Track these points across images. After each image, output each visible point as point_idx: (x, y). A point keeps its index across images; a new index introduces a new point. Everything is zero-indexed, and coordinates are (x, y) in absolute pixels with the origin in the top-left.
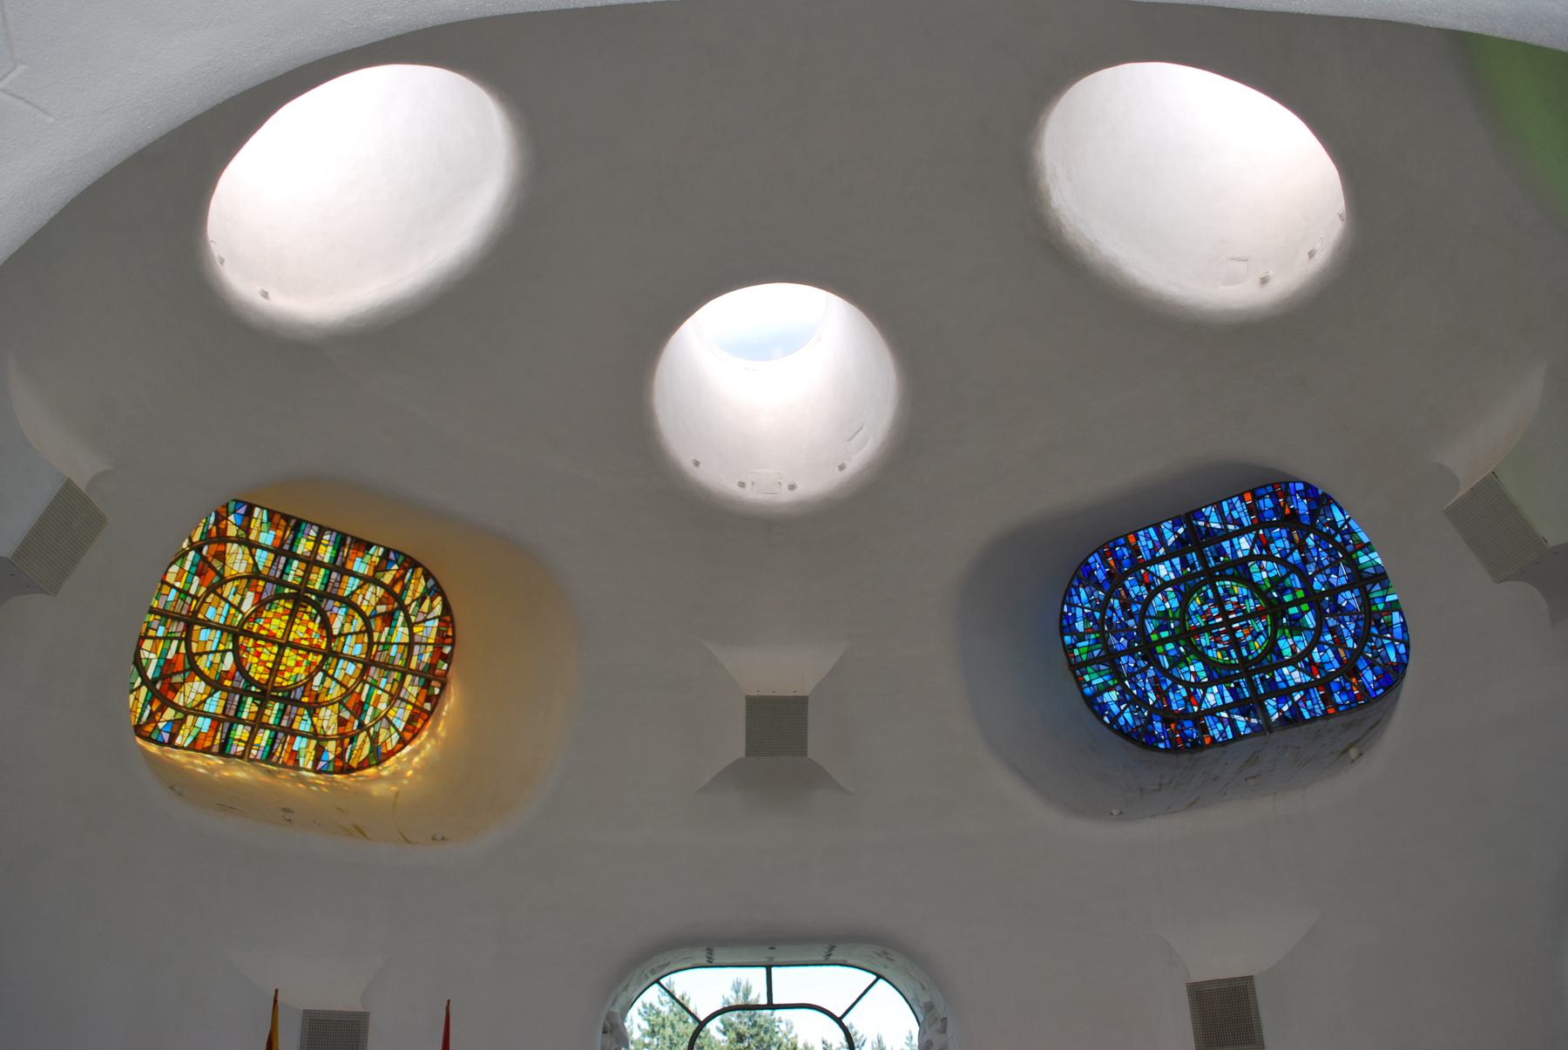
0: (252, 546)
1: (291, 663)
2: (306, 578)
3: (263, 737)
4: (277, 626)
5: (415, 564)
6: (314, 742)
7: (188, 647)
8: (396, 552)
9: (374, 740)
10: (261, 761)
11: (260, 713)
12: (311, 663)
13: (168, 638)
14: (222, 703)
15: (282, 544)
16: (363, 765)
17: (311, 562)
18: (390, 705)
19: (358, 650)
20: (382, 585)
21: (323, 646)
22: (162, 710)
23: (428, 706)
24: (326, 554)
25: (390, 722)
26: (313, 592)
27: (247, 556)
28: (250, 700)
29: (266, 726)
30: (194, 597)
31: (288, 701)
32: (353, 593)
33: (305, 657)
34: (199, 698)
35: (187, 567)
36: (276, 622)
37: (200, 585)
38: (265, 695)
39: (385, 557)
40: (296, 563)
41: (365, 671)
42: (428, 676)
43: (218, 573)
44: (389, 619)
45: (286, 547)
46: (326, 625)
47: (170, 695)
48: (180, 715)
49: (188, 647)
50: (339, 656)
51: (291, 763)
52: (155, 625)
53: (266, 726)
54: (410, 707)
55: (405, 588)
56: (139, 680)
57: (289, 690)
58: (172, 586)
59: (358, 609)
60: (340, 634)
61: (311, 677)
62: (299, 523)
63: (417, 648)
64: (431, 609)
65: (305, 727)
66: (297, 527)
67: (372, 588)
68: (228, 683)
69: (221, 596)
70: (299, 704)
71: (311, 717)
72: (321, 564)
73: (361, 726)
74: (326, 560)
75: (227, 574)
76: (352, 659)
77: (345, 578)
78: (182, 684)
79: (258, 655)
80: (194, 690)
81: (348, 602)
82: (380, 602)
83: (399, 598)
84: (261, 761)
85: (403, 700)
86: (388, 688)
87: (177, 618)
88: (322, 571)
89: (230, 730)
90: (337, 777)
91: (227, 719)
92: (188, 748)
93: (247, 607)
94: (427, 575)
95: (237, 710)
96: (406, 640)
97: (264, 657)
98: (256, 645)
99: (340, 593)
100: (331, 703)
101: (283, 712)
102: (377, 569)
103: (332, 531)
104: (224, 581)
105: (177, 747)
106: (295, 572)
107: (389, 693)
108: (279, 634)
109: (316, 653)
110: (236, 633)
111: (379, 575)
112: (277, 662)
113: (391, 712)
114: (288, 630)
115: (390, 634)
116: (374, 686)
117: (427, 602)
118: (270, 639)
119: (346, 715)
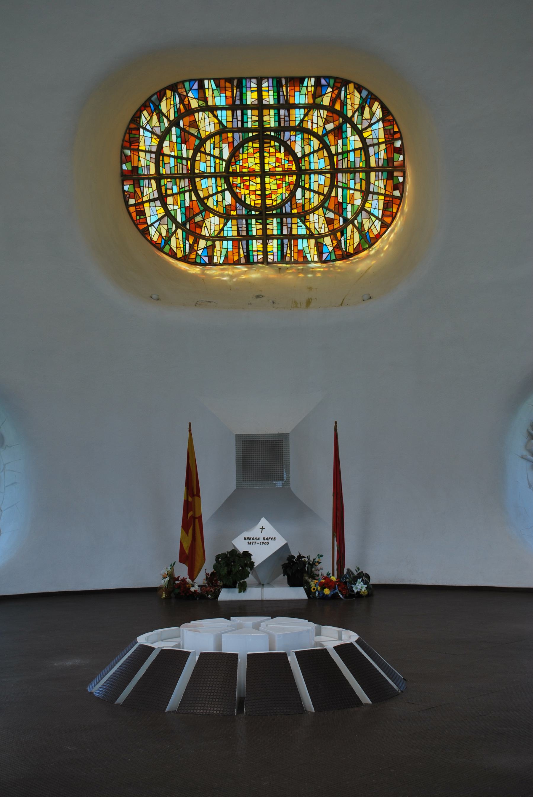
0: (213, 110)
1: (274, 187)
2: (261, 121)
3: (273, 246)
4: (253, 163)
5: (346, 83)
6: (313, 241)
7: (197, 195)
8: (325, 78)
9: (360, 229)
10: (278, 262)
11: (265, 229)
12: (289, 183)
13: (181, 192)
14: (235, 228)
15: (234, 101)
16: (358, 250)
17: (261, 107)
18: (365, 200)
19: (322, 164)
20: (324, 107)
21: (294, 168)
22: (196, 242)
23: (397, 193)
24: (270, 97)
25: (369, 213)
26: (270, 129)
27: (212, 119)
28: (254, 221)
29: (273, 237)
30: (187, 159)
31: (281, 216)
32: (302, 121)
33: (283, 180)
34: (218, 229)
35: (174, 140)
36: (251, 160)
37: (188, 149)
38: (263, 214)
39: (318, 84)
40: (249, 112)
41: (334, 178)
42: (389, 169)
43: (196, 137)
44: (339, 132)
45: (238, 102)
46: (290, 151)
47: (198, 231)
48: (210, 243)
49: (197, 195)
50: (310, 172)
51: (301, 259)
52: (169, 186)
53: (273, 237)
54: (382, 198)
55: (344, 104)
56: (174, 226)
57: (280, 206)
58: (170, 156)
59: (310, 132)
60: (304, 156)
61: (292, 194)
62: (240, 81)
63: (371, 150)
64: (372, 114)
65: (302, 231)
66: (239, 84)
67: (316, 113)
68: (233, 213)
69: (205, 153)
70: (291, 215)
71: (304, 223)
72: (269, 107)
73: (346, 220)
74: (272, 102)
75: (203, 136)
76: (321, 172)
77: (292, 111)
78: (203, 221)
79: (248, 187)
80: (212, 224)
81: (301, 129)
82: (327, 122)
83: (341, 114)
84: (278, 262)
85: (374, 193)
86: (358, 187)
87: (182, 177)
88: (272, 112)
89: (248, 245)
90: (338, 263)
91: (242, 239)
92: (224, 264)
93: (226, 155)
94: (359, 88)
95: (247, 231)
96: (361, 146)
97: (252, 188)
98: (243, 181)
99: (292, 124)
100: (316, 209)
101: (281, 224)
102: (315, 96)
103: (268, 78)
104: (203, 141)
105: (216, 265)
106: (251, 119)
107: (361, 191)
108: (258, 168)
109: (290, 175)
110: (226, 175)
111: (318, 100)
112: (263, 188)
113: (367, 205)
114: (262, 164)
115: (344, 144)
116: (346, 188)
117: (367, 109)
118: (252, 174)
119: (331, 215)
